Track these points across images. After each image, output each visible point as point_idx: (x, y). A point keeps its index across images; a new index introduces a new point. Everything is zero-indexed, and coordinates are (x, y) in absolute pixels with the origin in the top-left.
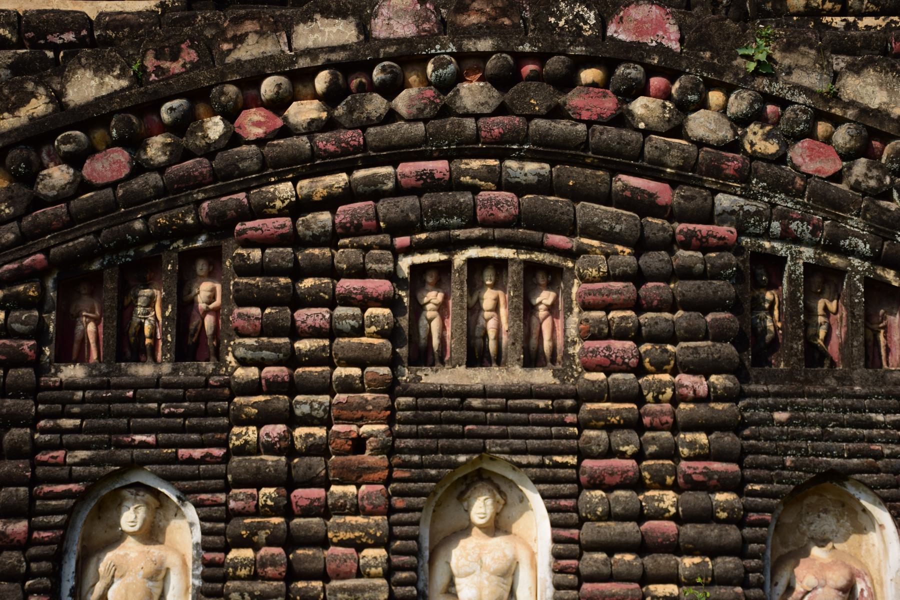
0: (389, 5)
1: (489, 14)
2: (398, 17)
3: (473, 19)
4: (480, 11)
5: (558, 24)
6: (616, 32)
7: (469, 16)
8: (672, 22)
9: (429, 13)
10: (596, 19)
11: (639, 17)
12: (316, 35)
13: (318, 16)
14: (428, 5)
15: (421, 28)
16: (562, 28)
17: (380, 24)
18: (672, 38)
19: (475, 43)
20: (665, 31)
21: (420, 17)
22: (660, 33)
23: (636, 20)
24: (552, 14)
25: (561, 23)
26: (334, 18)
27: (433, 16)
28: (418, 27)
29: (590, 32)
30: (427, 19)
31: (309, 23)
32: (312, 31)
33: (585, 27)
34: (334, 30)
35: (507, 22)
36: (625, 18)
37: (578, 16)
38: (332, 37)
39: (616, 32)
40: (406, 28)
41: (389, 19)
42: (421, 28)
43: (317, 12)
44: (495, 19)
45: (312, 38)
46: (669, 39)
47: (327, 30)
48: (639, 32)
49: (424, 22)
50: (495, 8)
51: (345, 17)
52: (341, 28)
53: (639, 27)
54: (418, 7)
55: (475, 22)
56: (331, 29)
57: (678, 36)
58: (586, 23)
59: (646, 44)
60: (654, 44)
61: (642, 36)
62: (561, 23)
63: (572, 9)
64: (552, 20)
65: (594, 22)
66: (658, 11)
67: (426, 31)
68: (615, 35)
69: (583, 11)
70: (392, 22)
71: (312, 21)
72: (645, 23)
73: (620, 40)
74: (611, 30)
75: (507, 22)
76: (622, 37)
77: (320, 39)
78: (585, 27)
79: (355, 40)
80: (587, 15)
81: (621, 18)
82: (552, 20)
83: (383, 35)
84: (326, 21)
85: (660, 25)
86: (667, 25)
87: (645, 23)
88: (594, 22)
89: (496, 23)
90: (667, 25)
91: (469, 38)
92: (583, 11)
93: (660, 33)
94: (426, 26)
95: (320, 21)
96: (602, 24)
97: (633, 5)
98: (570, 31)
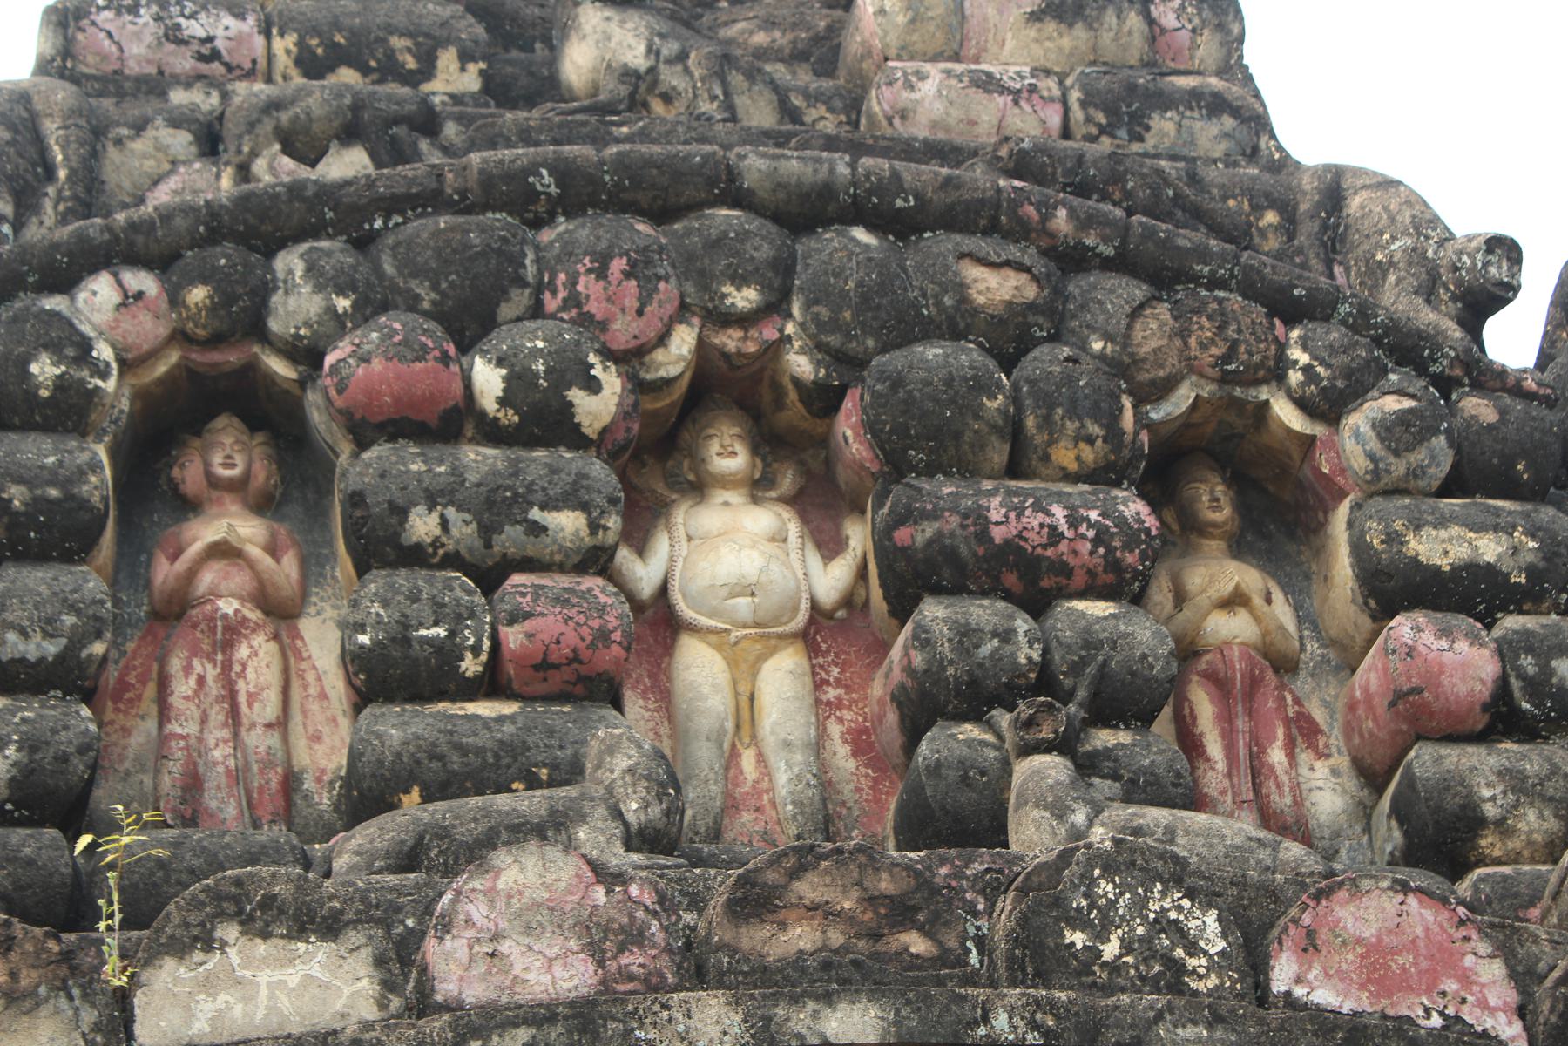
0: (493, 889)
1: (850, 919)
2: (528, 929)
3: (801, 937)
4: (823, 912)
5: (1099, 954)
6: (1298, 980)
7: (783, 926)
8: (1484, 948)
9: (640, 914)
10: (1224, 936)
11: (1368, 932)
12: (222, 998)
13: (229, 932)
14: (634, 890)
15: (612, 966)
16: (1114, 967)
17: (463, 954)
18: (1493, 1001)
19: (815, 1015)
20: (1466, 979)
21: (606, 930)
22: (1451, 986)
23: (1359, 941)
24: (1078, 921)
25: (1110, 950)
26: (288, 937)
27: (655, 926)
28: (601, 964)
29: (1213, 981)
30: (634, 937)
31: (198, 956)
32: (209, 985)
33: (1192, 962)
34: (293, 976)
35: (918, 944)
36: (1323, 935)
37: (1161, 924)
38: (285, 1003)
39: (1298, 980)
40: (558, 971)
41: (496, 937)
42: (612, 966)
43: (231, 917)
44: (876, 936)
45: (206, 1008)
46: (1483, 1005)
47: (265, 977)
48: (1379, 982)
49: (622, 949)
50: (871, 900)
51: (331, 929)
52: (316, 971)
53: (1375, 965)
54: (599, 895)
55: (806, 944)
56: (277, 976)
57: (1513, 997)
58: (1193, 949)
59: (1410, 1020)
60: (1436, 1021)
61: (1390, 995)
62: (1110, 950)
63: (1141, 905)
64: (1078, 939)
65: (1221, 945)
66: (1429, 915)
67: (631, 978)
68: (1299, 992)
69: (1180, 909)
70: (504, 947)
71: (208, 947)
72: (1394, 951)
73: (1319, 1010)
74: (1283, 974)
75: (918, 944)
76: (1324, 997)
77: (238, 1010)
78: (1192, 962)
79: (370, 1012)
80: (1192, 924)
81: (1310, 934)
82: (1078, 939)
83: (475, 993)
84: (261, 947)
85: (1444, 960)
86: (1469, 960)
87: (1394, 951)
88: (1221, 945)
89: (881, 947)
90: (1469, 960)
91: (795, 1000)
92: (1180, 909)
93: (1451, 986)
94: (633, 960)
95: (238, 950)
96: (1252, 959)
97: (1342, 894)
98: (1143, 978)
